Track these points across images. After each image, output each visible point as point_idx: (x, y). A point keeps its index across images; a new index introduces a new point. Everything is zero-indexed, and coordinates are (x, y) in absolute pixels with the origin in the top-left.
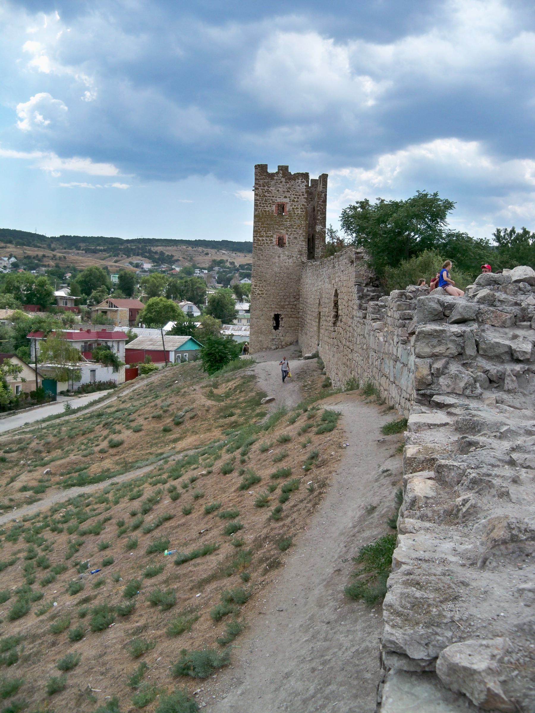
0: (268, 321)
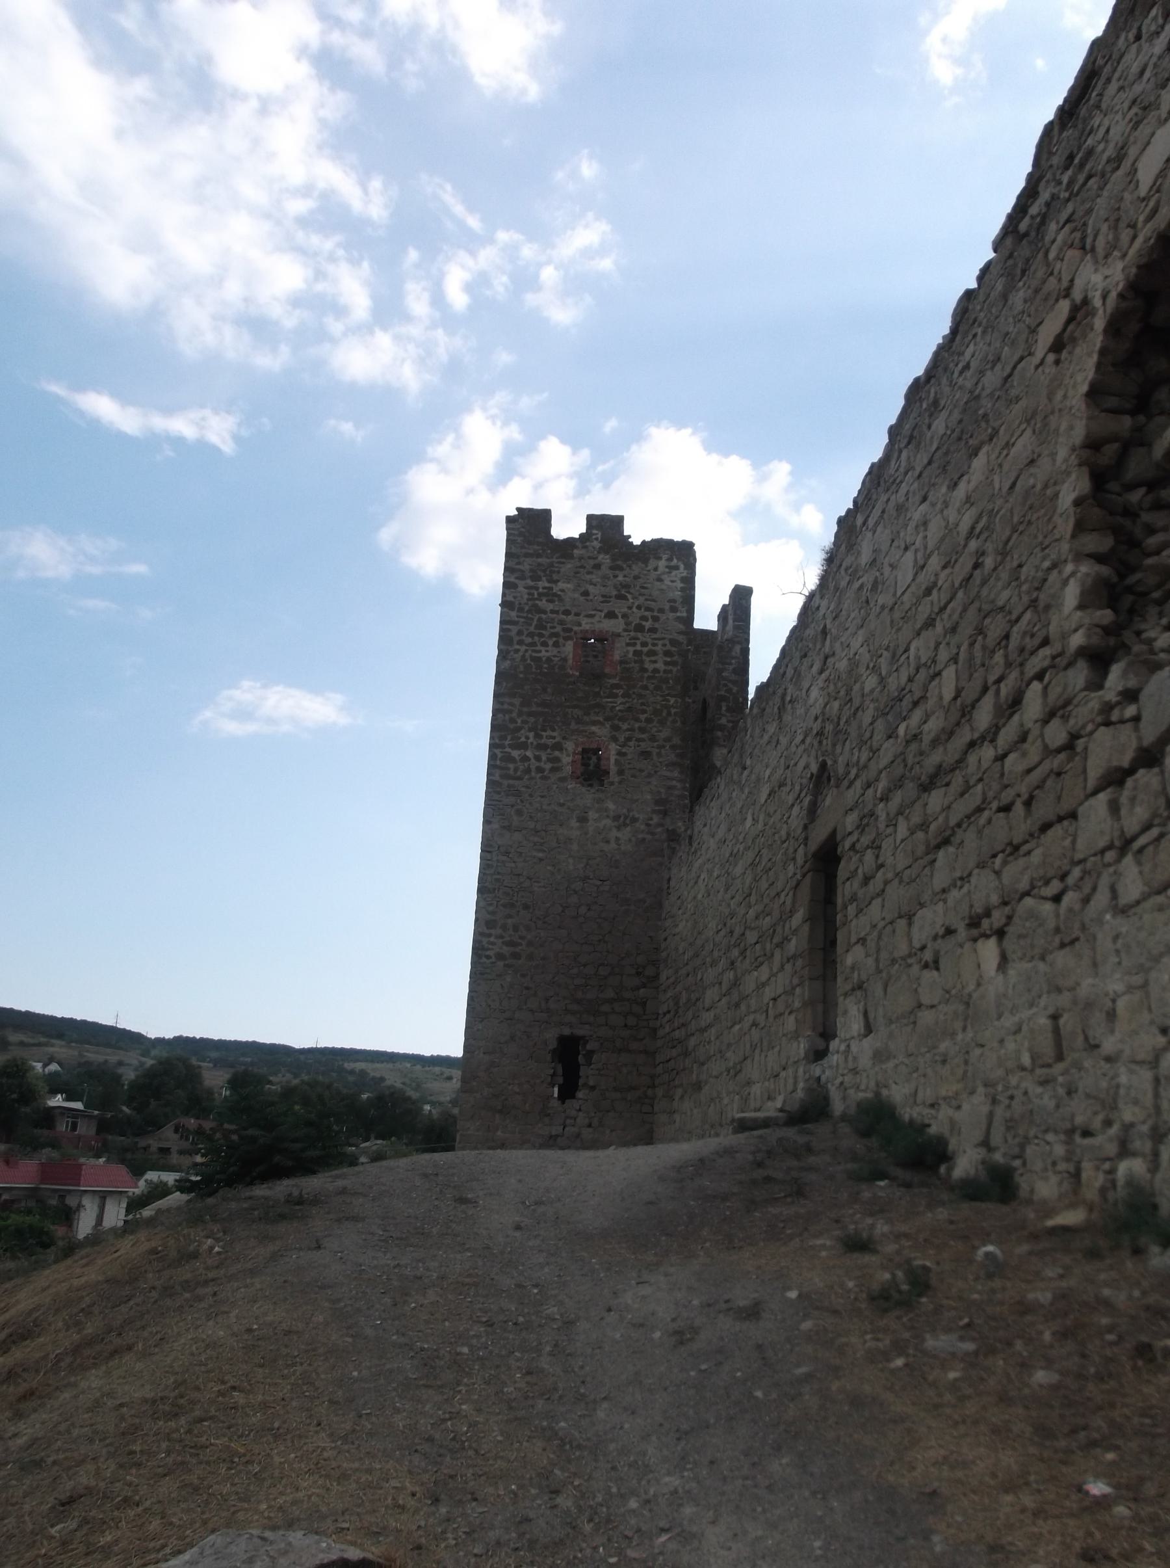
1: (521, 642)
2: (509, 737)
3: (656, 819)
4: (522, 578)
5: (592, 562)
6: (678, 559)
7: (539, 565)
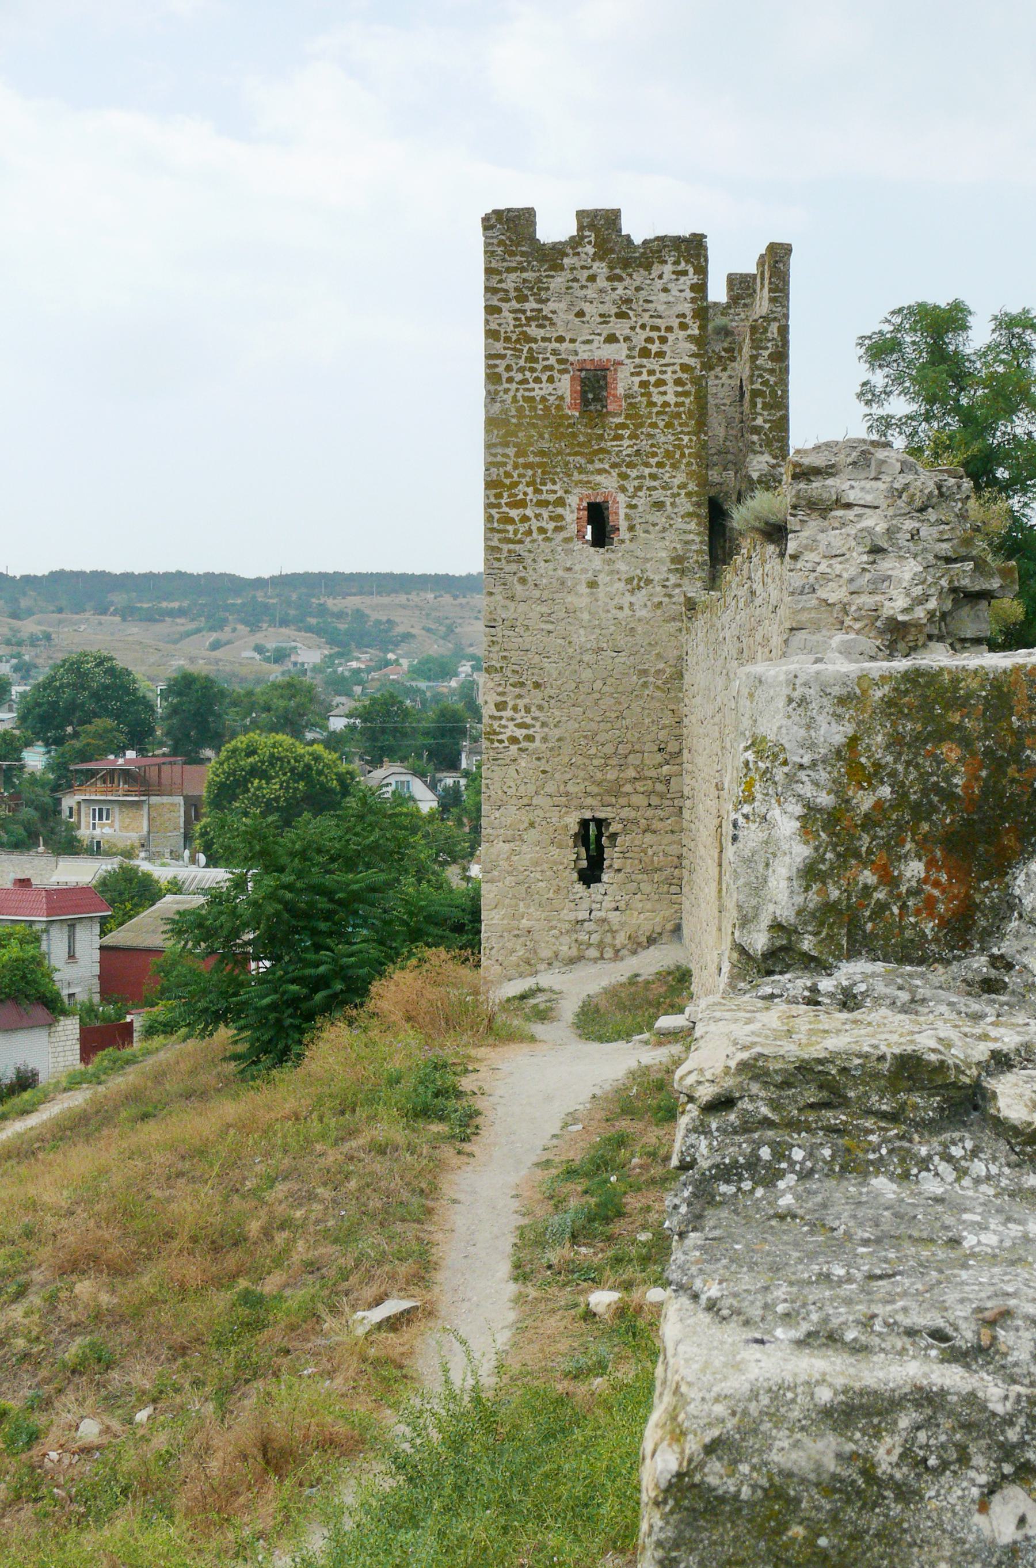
0: (554, 851)
1: (510, 380)
2: (505, 495)
3: (673, 579)
4: (507, 300)
5: (586, 273)
6: (687, 262)
7: (525, 281)
